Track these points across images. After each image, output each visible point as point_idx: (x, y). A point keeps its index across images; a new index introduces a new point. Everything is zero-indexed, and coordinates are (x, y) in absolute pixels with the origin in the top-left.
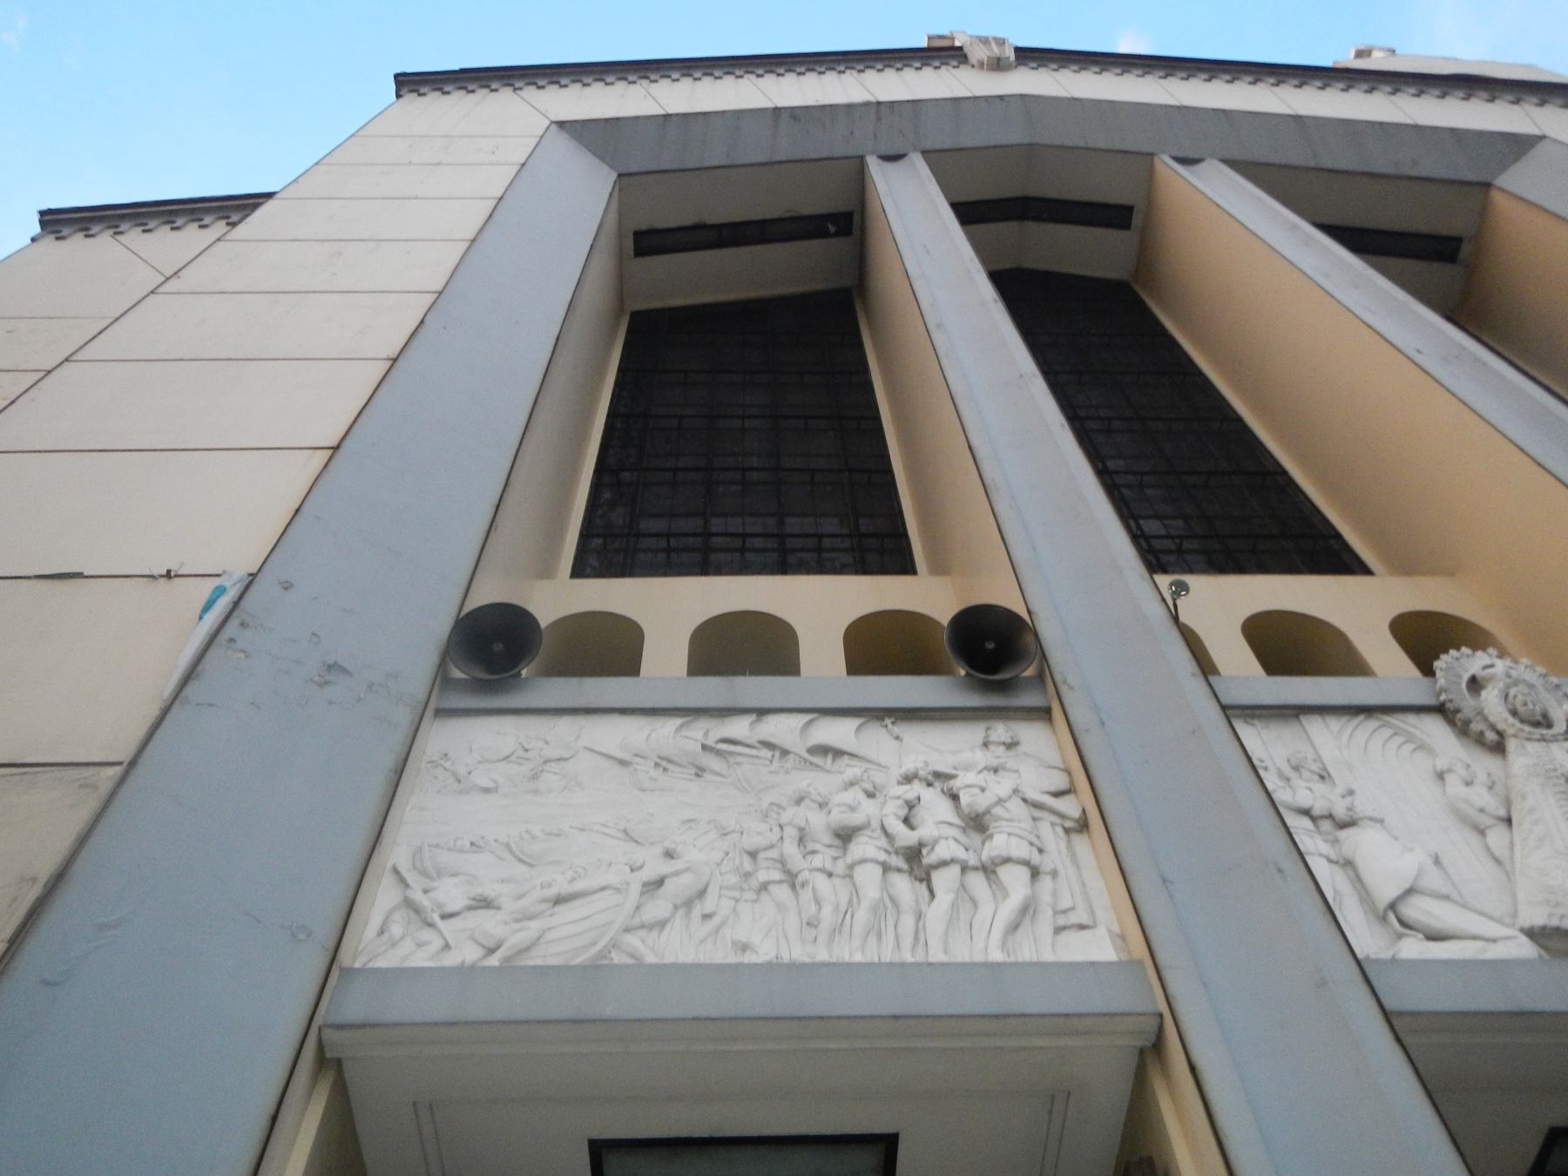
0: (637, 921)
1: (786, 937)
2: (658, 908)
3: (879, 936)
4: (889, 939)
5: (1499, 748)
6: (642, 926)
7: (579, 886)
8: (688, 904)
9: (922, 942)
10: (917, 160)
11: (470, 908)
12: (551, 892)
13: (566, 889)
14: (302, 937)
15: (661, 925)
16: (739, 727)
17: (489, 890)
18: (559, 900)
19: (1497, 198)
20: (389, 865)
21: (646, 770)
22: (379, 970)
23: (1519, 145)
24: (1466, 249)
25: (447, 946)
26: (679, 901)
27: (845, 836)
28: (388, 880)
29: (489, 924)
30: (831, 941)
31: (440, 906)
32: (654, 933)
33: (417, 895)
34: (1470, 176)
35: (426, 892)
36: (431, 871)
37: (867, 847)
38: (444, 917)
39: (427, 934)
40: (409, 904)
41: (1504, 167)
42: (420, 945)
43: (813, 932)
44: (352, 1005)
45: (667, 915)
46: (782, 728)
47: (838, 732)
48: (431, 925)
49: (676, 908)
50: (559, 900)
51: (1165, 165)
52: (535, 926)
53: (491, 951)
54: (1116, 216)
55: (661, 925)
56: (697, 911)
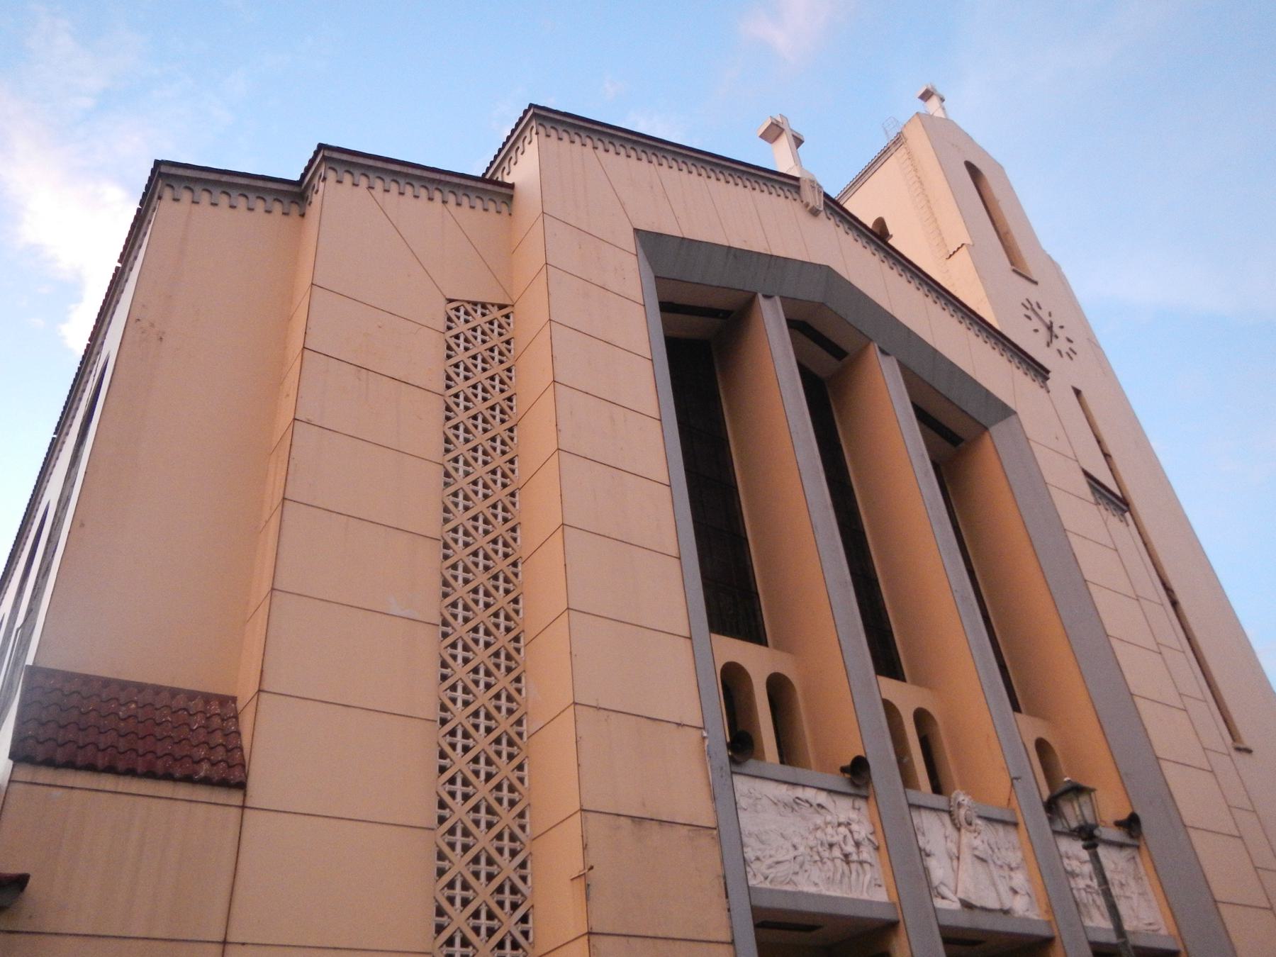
5: (959, 830)
10: (777, 298)
12: (775, 859)
16: (799, 792)
19: (987, 436)
21: (781, 806)
23: (1006, 412)
24: (962, 445)
27: (831, 846)
34: (983, 421)
37: (837, 852)
41: (996, 421)
46: (809, 794)
47: (822, 798)
50: (778, 863)
51: (874, 349)
53: (766, 878)
54: (837, 352)
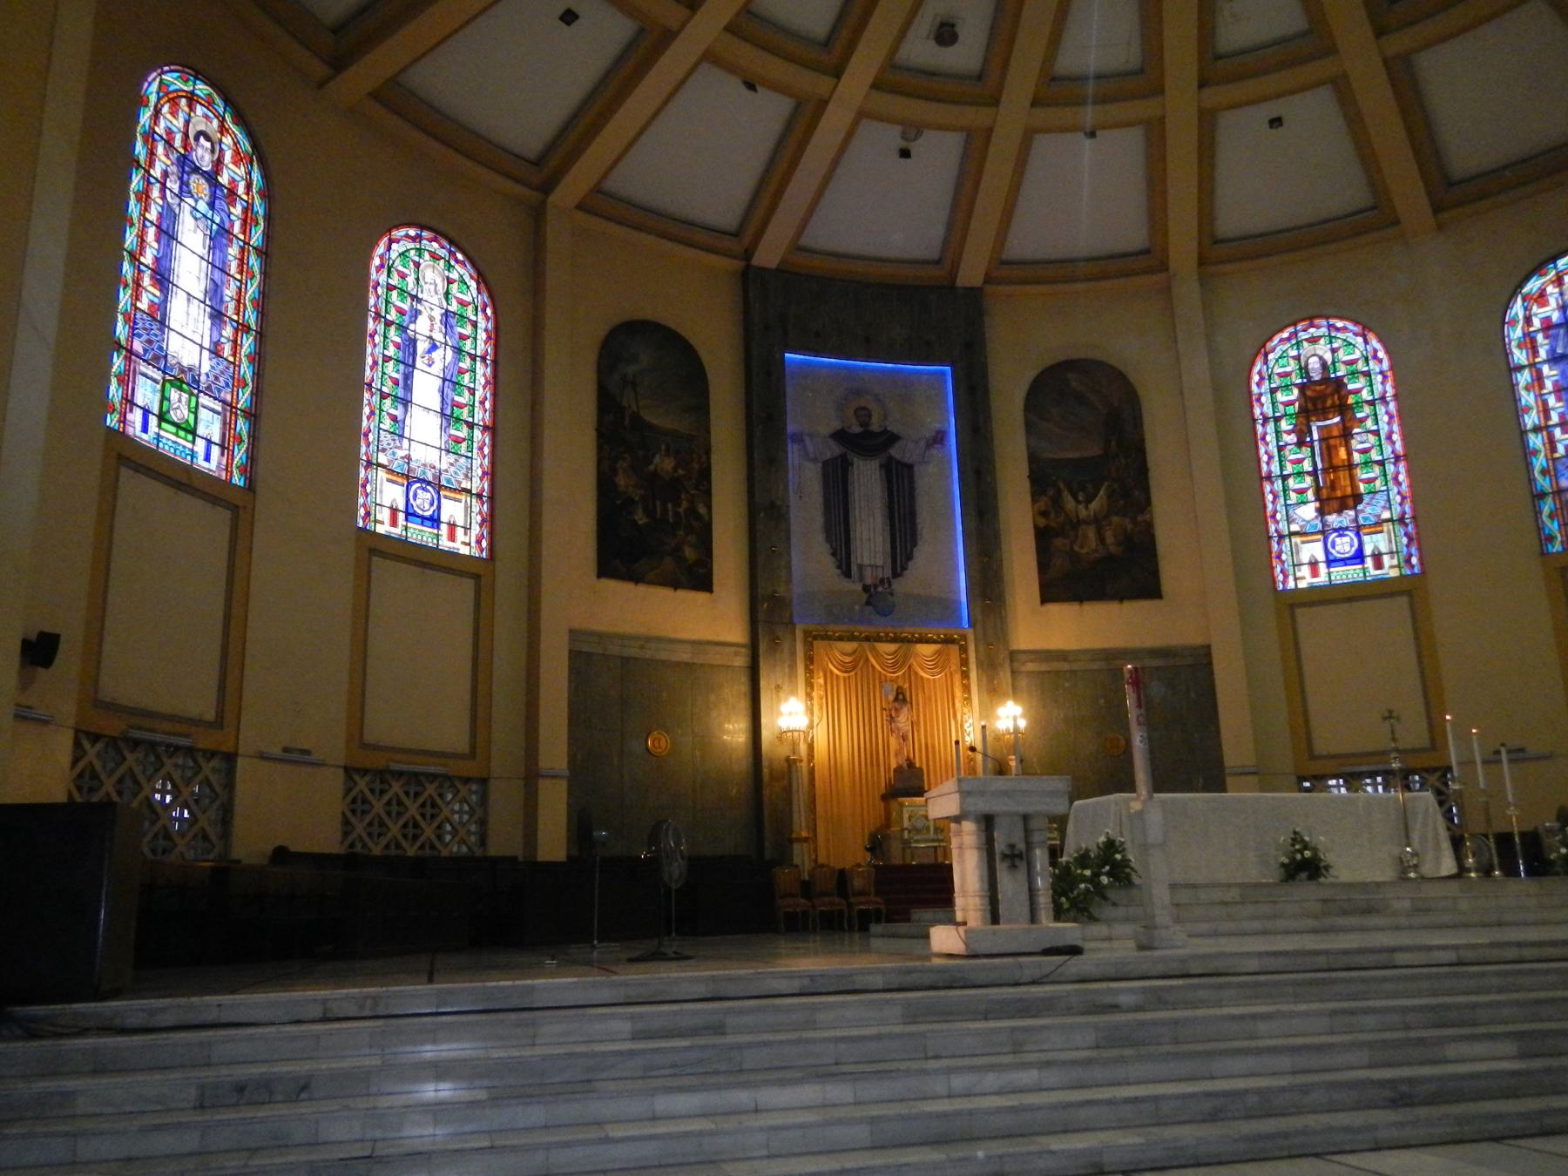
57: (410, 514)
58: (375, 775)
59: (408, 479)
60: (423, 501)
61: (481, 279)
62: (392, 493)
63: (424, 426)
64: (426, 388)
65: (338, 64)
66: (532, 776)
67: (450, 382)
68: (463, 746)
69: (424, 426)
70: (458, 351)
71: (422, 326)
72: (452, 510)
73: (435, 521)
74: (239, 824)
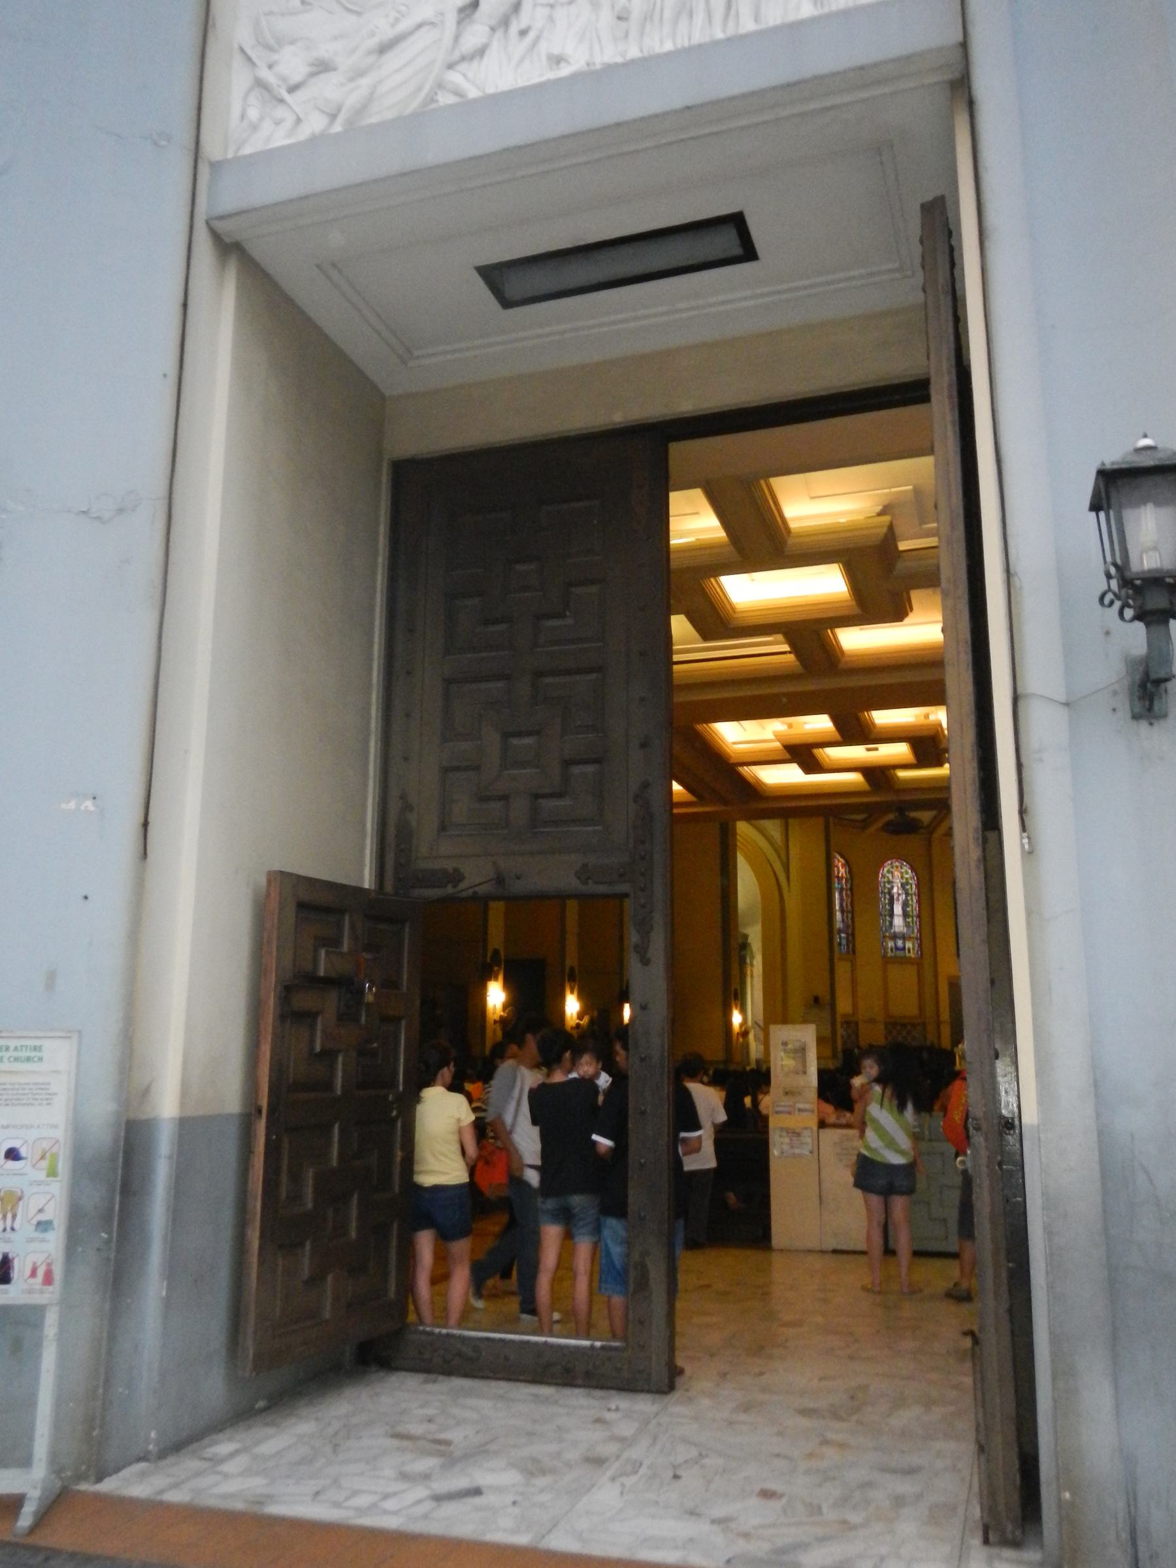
0: (457, 55)
1: (599, 38)
2: (475, 34)
3: (691, 15)
4: (700, 17)
6: (463, 59)
7: (404, 26)
8: (505, 22)
9: (733, 12)
11: (313, 75)
12: (373, 42)
13: (390, 33)
14: (163, 143)
15: (481, 52)
17: (325, 50)
18: (384, 49)
20: (236, 46)
22: (245, 157)
25: (299, 120)
26: (493, 22)
28: (238, 61)
29: (328, 88)
30: (642, 34)
31: (284, 79)
32: (475, 62)
33: (265, 74)
35: (270, 67)
36: (272, 42)
38: (292, 89)
39: (280, 112)
40: (260, 84)
42: (278, 123)
43: (623, 25)
44: (228, 197)
45: (484, 40)
48: (281, 101)
49: (493, 29)
50: (384, 49)
52: (365, 82)
53: (333, 117)
55: (481, 52)
56: (514, 28)
57: (897, 948)
58: (893, 1024)
59: (894, 937)
60: (900, 943)
61: (913, 869)
62: (891, 944)
63: (898, 922)
64: (898, 909)
65: (864, 828)
66: (938, 1024)
67: (905, 905)
68: (915, 1012)
69: (898, 922)
70: (907, 894)
71: (895, 890)
72: (909, 945)
73: (904, 949)
74: (861, 1039)
